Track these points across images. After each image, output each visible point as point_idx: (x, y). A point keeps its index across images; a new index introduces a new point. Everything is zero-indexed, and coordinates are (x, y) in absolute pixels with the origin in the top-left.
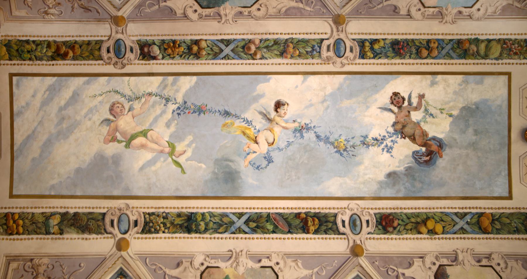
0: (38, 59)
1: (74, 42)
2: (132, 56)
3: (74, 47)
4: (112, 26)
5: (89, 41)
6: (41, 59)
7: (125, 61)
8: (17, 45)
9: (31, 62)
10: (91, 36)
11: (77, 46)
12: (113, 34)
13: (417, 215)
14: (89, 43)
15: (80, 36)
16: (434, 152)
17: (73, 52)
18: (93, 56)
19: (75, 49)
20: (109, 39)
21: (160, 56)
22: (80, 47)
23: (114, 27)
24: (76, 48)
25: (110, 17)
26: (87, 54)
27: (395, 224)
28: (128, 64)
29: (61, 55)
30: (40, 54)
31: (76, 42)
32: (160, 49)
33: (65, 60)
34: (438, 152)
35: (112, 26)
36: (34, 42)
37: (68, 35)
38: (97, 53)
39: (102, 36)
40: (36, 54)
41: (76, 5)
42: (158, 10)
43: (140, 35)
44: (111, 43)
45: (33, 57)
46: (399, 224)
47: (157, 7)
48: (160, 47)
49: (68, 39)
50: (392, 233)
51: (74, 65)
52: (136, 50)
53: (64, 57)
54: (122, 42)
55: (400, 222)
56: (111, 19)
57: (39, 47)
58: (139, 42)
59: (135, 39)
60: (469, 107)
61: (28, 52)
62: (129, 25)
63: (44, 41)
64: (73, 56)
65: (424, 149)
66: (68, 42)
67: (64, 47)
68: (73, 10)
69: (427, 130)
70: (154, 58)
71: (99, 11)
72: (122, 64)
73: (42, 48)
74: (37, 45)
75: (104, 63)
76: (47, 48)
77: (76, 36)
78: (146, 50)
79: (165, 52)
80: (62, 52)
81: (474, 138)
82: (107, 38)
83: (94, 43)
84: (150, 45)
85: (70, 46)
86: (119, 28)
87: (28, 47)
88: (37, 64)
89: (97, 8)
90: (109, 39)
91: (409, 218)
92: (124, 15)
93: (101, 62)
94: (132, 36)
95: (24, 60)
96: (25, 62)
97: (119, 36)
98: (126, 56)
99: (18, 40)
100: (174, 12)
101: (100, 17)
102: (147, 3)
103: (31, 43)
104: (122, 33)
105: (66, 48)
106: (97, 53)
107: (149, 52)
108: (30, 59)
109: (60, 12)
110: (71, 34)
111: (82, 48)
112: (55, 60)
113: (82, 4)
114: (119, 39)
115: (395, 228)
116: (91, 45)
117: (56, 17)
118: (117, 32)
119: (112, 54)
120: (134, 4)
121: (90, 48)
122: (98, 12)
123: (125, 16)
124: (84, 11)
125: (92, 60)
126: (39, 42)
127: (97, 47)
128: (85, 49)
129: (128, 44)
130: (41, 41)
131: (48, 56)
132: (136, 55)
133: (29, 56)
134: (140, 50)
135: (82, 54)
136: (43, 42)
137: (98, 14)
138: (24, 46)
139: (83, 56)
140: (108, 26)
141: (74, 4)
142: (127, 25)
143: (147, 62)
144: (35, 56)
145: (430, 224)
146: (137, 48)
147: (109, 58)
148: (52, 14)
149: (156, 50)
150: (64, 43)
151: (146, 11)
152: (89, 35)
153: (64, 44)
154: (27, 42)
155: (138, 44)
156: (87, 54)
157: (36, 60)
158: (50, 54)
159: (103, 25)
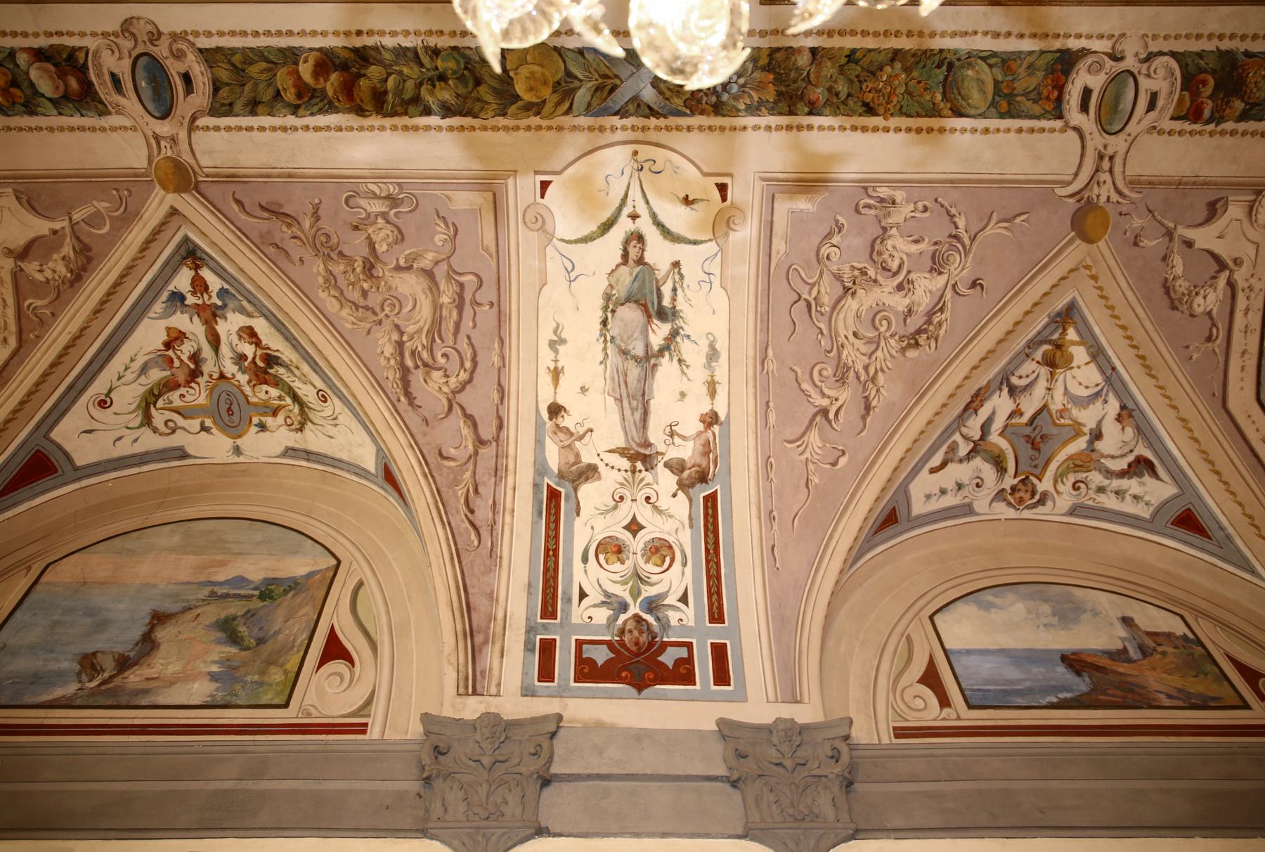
0: (410, 55)
1: (301, 111)
2: (110, 62)
3: (299, 95)
4: (192, 161)
5: (253, 113)
6: (401, 52)
7: (127, 44)
8: (479, 100)
9: (433, 41)
10: (249, 129)
11: (290, 96)
12: (183, 135)
14: (253, 107)
15: (285, 129)
17: (299, 78)
18: (233, 65)
19: (295, 86)
20: (194, 119)
21: (22, 59)
22: (278, 93)
23: (186, 157)
24: (292, 90)
25: (202, 187)
26: (253, 70)
28: (115, 34)
29: (336, 68)
30: (406, 71)
31: (295, 110)
32: (32, 84)
33: (320, 50)
35: (192, 161)
36: (427, 112)
37: (323, 133)
38: (224, 74)
39: (217, 129)
40: (416, 69)
41: (307, 224)
42: (73, 208)
43: (103, 129)
44: (185, 106)
45: (426, 60)
47: (76, 217)
48: (37, 93)
49: (321, 120)
51: (290, 33)
52: (103, 83)
53: (327, 61)
54: (151, 107)
56: (197, 182)
57: (408, 95)
58: (103, 110)
59: (115, 120)
61: (442, 78)
62: (145, 164)
63: (393, 114)
64: (296, 64)
66: (320, 111)
67: (330, 94)
68: (316, 209)
70: (39, 55)
71: (236, 207)
72: (133, 35)
73: (399, 91)
74: (416, 100)
75: (191, 38)
76: (386, 92)
77: (296, 129)
78: (74, 84)
79: (14, 75)
80: (334, 77)
82: (201, 122)
83: (238, 107)
84: (66, 97)
85: (312, 97)
86: (169, 153)
87: (446, 95)
88: (412, 37)
89: (243, 217)
90: (194, 119)
92: (162, 192)
93: (203, 43)
94: (125, 128)
95: (455, 48)
96: (453, 42)
97: (164, 128)
98: (127, 63)
99: (475, 117)
100: (24, 201)
101: (232, 187)
102: (106, 229)
103: (434, 107)
104: (157, 138)
105: (324, 90)
106: (224, 74)
107: (62, 75)
108: (436, 52)
109: (351, 202)
110: (311, 134)
111: (271, 92)
112: (355, 51)
113: (289, 226)
114: (163, 117)
116: (243, 100)
117: (363, 188)
118: (174, 140)
119: (174, 69)
120: (141, 223)
121: (247, 88)
122: (238, 202)
123: (158, 191)
124: (281, 206)
125: (233, 51)
126: (411, 109)
127: (224, 92)
128: (261, 86)
129: (130, 103)
130: (406, 113)
131: (380, 62)
132: (98, 66)
133: (439, 63)
134: (91, 84)
135: (269, 70)
136: (399, 109)
137: (237, 196)
138: (458, 95)
139: (264, 65)
140: (205, 161)
141: (312, 227)
142: (150, 163)
143: (55, 41)
144: (421, 65)
146: (104, 91)
147: (179, 56)
148: (376, 196)
149: (42, 80)
150: (330, 107)
151: (106, 205)
152: (256, 133)
153: (330, 103)
154: (447, 111)
155: (102, 102)
156: (253, 70)
157: (415, 51)
158: (374, 71)
159: (218, 163)
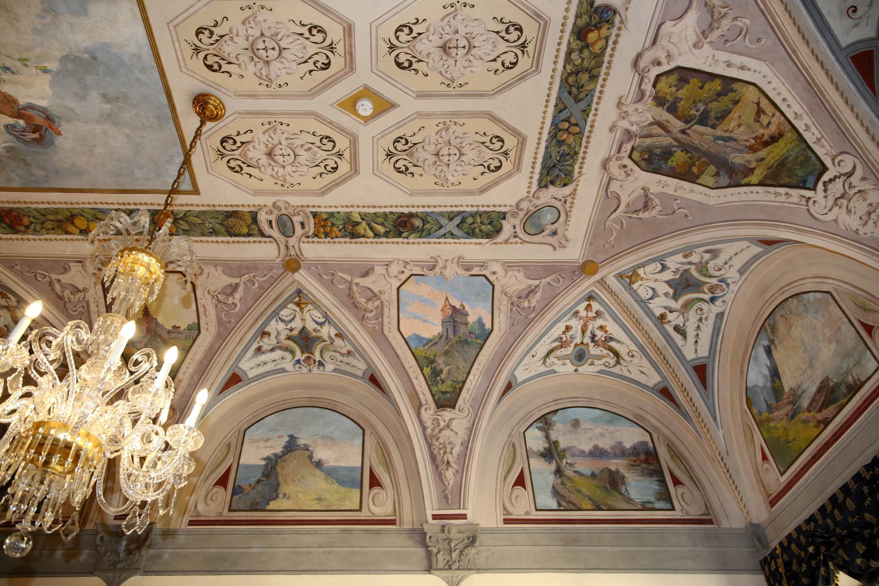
13: (56, 211)
16: (42, 126)
27: (26, 221)
34: (51, 127)
46: (32, 223)
50: (25, 232)
55: (32, 220)
60: (76, 57)
65: (22, 122)
69: (12, 94)
81: (107, 107)
91: (44, 215)
115: (27, 227)
145: (81, 223)
